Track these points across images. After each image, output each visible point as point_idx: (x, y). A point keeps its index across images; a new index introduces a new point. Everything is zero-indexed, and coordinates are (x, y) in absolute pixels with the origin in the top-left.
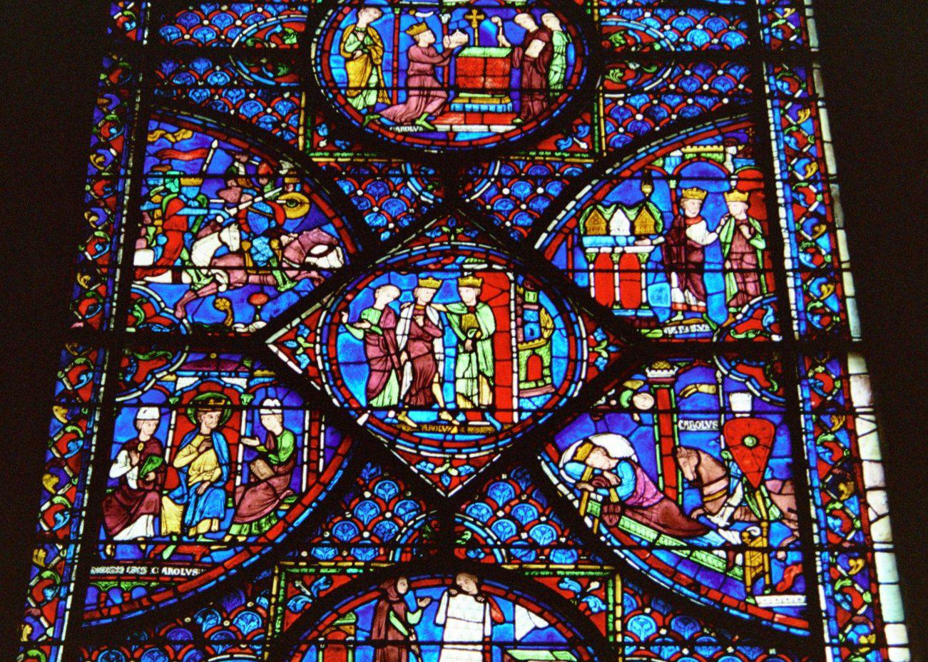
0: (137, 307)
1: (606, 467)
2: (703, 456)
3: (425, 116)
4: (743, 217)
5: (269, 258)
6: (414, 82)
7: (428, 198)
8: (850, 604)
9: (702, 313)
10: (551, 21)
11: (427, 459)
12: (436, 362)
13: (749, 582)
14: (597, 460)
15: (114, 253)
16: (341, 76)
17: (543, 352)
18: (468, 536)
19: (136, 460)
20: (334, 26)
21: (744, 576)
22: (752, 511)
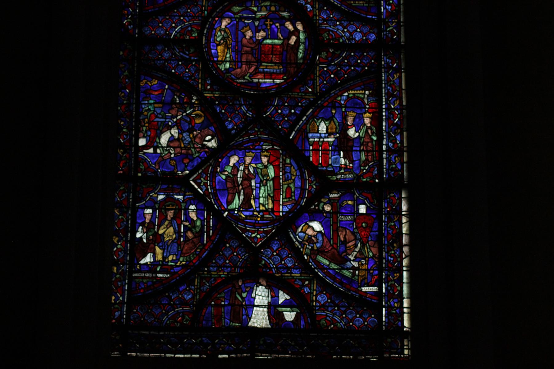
0: (141, 164)
1: (313, 235)
2: (347, 231)
3: (248, 75)
4: (369, 125)
5: (190, 142)
6: (244, 59)
7: (249, 114)
8: (393, 291)
9: (351, 169)
10: (300, 27)
11: (249, 231)
12: (252, 190)
13: (360, 282)
14: (310, 232)
15: (131, 139)
16: (215, 53)
17: (292, 186)
18: (263, 262)
19: (145, 230)
20: (212, 28)
21: (358, 279)
22: (363, 254)
